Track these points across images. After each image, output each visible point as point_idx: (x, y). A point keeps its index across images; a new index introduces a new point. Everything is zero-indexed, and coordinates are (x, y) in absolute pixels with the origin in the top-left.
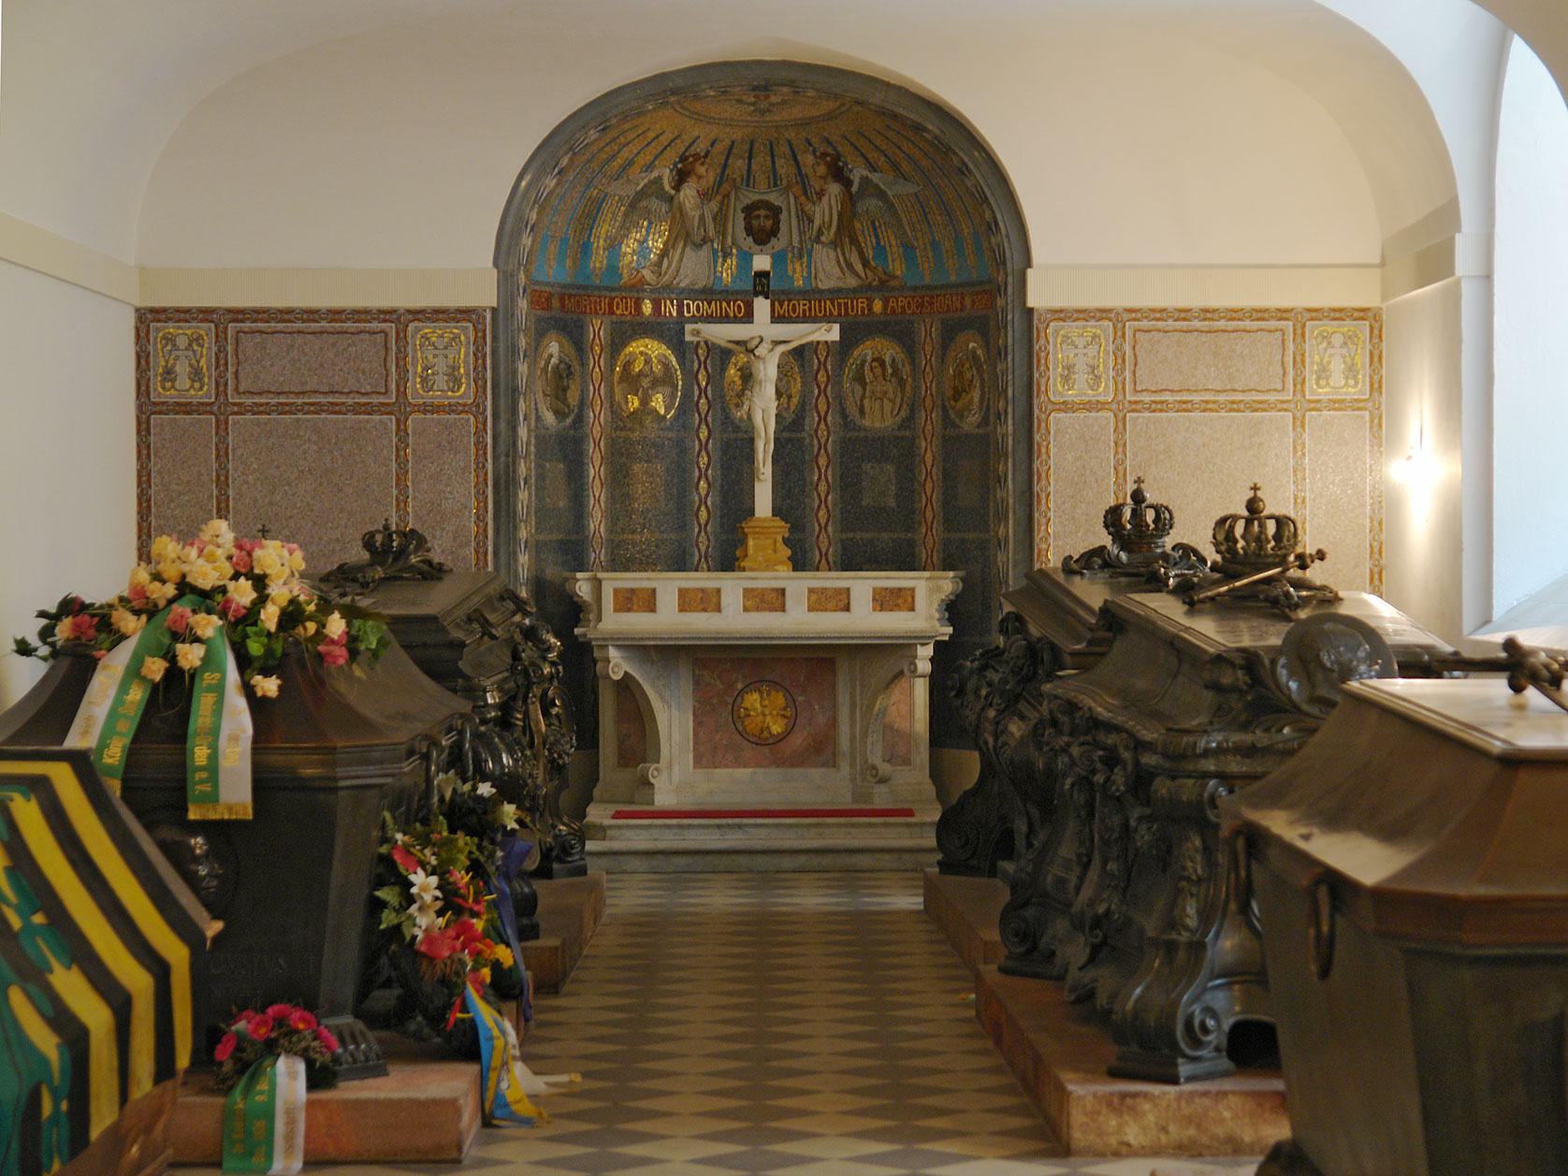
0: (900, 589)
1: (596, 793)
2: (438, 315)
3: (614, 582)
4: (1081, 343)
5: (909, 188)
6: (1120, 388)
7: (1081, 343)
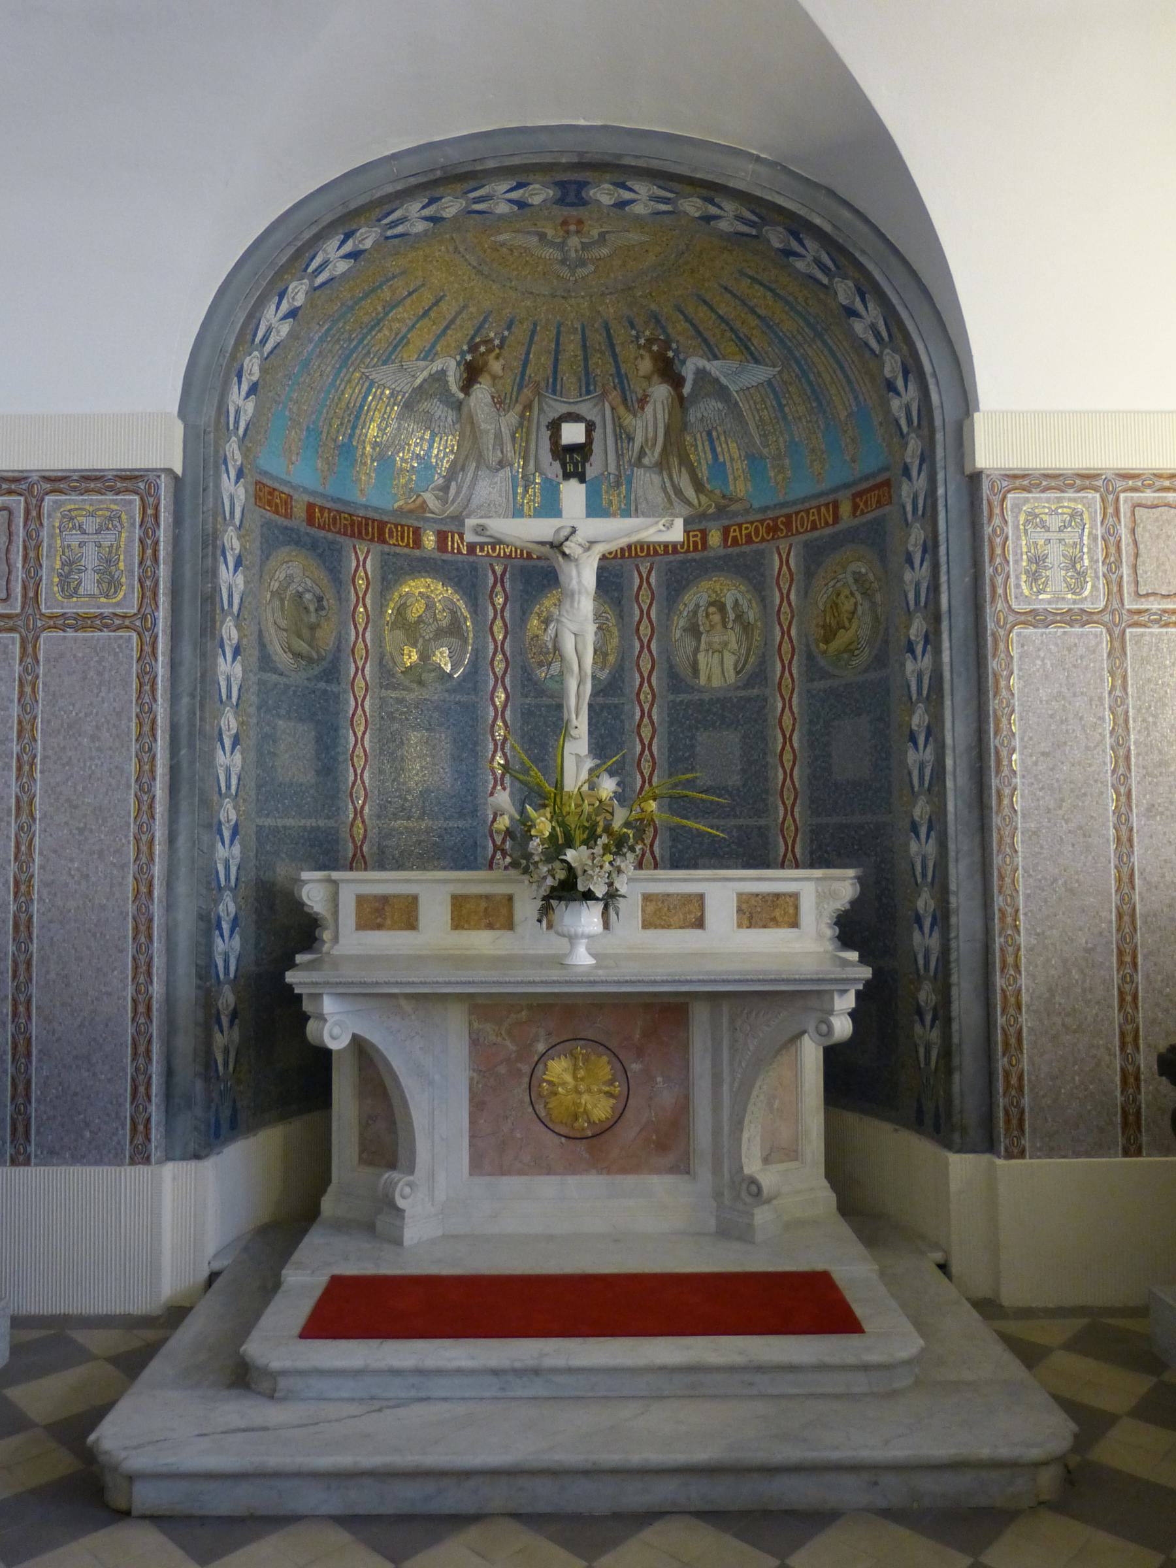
0: (777, 896)
1: (328, 1205)
2: (91, 481)
3: (358, 884)
4: (1054, 522)
5: (761, 374)
6: (1115, 589)
7: (1054, 522)
